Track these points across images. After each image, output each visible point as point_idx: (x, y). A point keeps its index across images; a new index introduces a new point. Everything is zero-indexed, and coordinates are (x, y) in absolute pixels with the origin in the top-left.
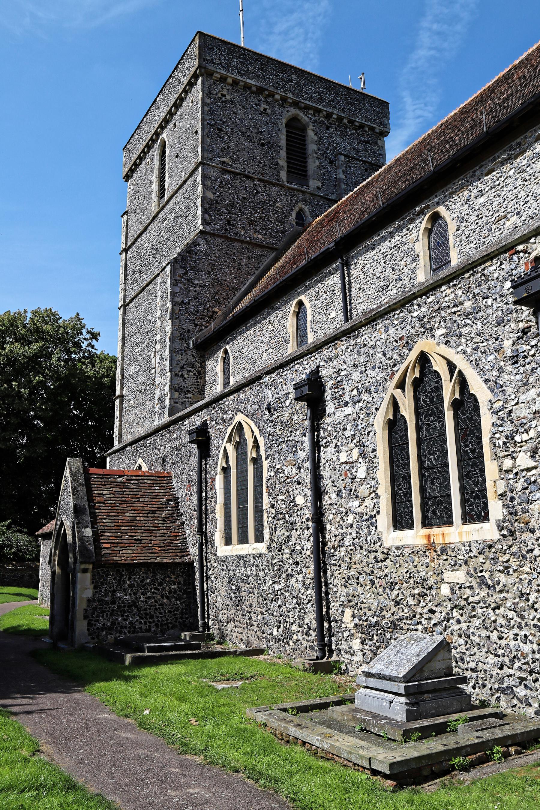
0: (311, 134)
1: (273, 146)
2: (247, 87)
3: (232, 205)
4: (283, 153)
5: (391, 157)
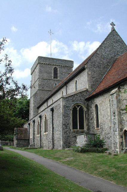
0: (58, 70)
4: (53, 74)
5: (73, 70)
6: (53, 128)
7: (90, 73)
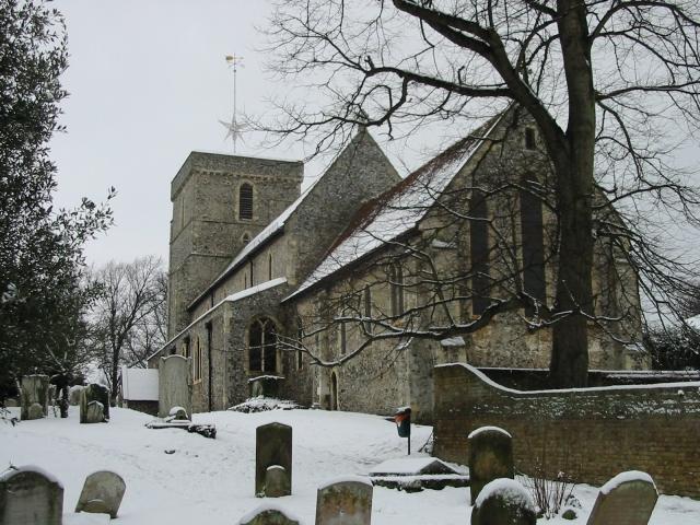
0: (255, 192)
1: (231, 202)
2: (218, 174)
3: (208, 238)
4: (238, 206)
6: (211, 368)
7: (294, 243)
